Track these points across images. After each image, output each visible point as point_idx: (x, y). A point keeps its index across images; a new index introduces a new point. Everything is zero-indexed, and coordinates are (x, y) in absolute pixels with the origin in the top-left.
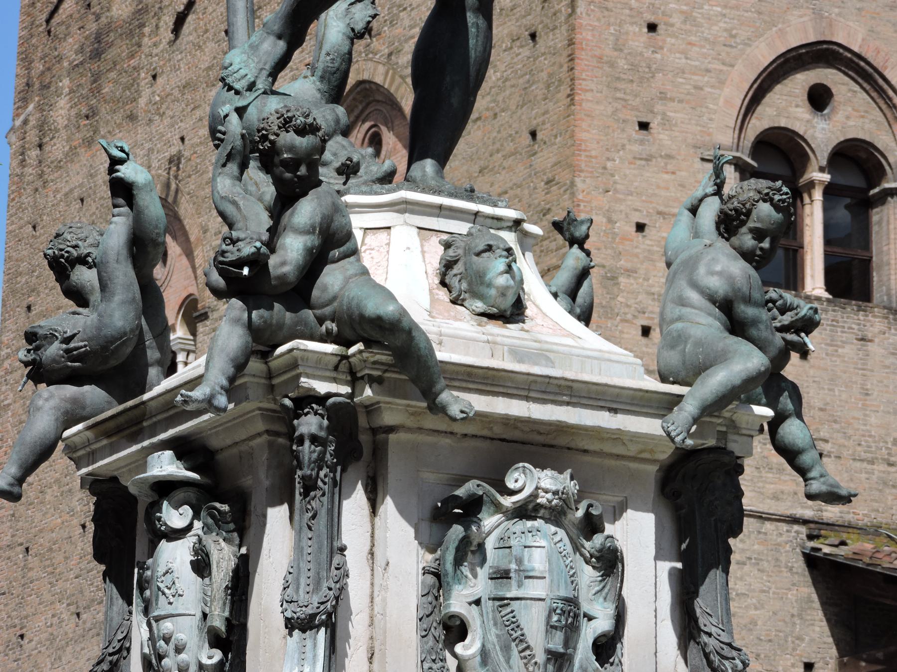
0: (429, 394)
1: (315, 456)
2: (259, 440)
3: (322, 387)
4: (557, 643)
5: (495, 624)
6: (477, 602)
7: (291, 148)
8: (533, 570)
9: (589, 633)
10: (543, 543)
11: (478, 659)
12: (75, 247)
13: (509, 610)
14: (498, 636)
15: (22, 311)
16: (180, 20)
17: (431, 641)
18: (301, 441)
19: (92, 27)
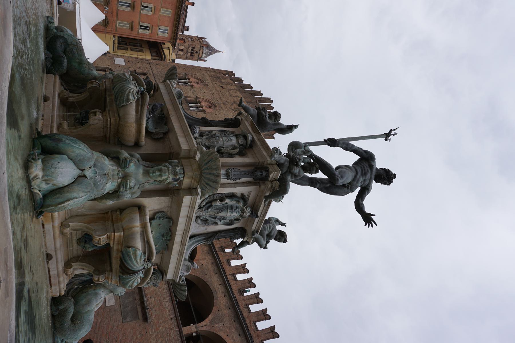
1: (259, 175)
2: (257, 160)
3: (271, 176)
5: (222, 207)
7: (313, 170)
8: (232, 213)
9: (218, 221)
10: (237, 215)
11: (216, 204)
12: (278, 117)
13: (225, 209)
14: (220, 207)
15: (191, 67)
16: (222, 87)
18: (262, 172)
19: (221, 77)
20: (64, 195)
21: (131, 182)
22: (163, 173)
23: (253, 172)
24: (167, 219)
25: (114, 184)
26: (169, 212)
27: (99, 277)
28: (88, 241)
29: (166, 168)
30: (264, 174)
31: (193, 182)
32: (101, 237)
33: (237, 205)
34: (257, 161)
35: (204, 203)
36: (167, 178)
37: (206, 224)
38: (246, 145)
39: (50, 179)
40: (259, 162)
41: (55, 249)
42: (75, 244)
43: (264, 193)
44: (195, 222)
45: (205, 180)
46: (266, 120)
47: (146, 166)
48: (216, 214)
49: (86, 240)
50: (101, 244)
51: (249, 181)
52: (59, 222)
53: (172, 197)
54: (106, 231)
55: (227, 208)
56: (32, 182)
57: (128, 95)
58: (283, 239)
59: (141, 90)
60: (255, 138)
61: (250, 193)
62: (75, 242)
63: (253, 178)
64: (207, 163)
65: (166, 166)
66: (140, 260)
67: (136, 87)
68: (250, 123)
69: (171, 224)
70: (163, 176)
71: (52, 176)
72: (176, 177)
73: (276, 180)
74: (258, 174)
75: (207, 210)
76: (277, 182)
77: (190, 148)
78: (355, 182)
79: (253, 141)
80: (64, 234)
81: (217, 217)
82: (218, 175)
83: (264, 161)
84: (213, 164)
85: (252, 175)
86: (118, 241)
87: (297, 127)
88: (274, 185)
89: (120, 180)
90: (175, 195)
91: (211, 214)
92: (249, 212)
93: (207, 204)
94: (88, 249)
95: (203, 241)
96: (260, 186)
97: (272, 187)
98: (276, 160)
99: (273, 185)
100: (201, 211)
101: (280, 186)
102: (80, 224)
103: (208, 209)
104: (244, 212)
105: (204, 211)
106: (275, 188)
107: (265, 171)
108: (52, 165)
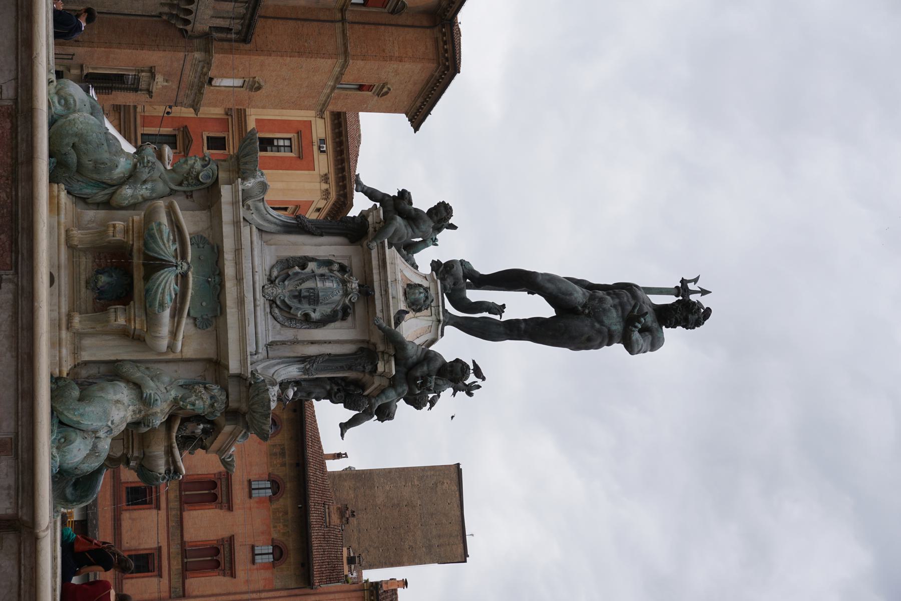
0: (374, 239)
3: (370, 219)
4: (304, 293)
6: (313, 272)
8: (326, 282)
11: (295, 271)
25: (129, 162)
26: (211, 236)
27: (115, 308)
31: (231, 177)
35: (275, 273)
39: (62, 87)
41: (59, 267)
44: (269, 316)
48: (298, 286)
55: (313, 276)
58: (461, 365)
62: (83, 283)
66: (168, 242)
78: (597, 302)
86: (139, 232)
91: (290, 289)
92: (357, 280)
96: (362, 246)
100: (274, 287)
103: (283, 281)
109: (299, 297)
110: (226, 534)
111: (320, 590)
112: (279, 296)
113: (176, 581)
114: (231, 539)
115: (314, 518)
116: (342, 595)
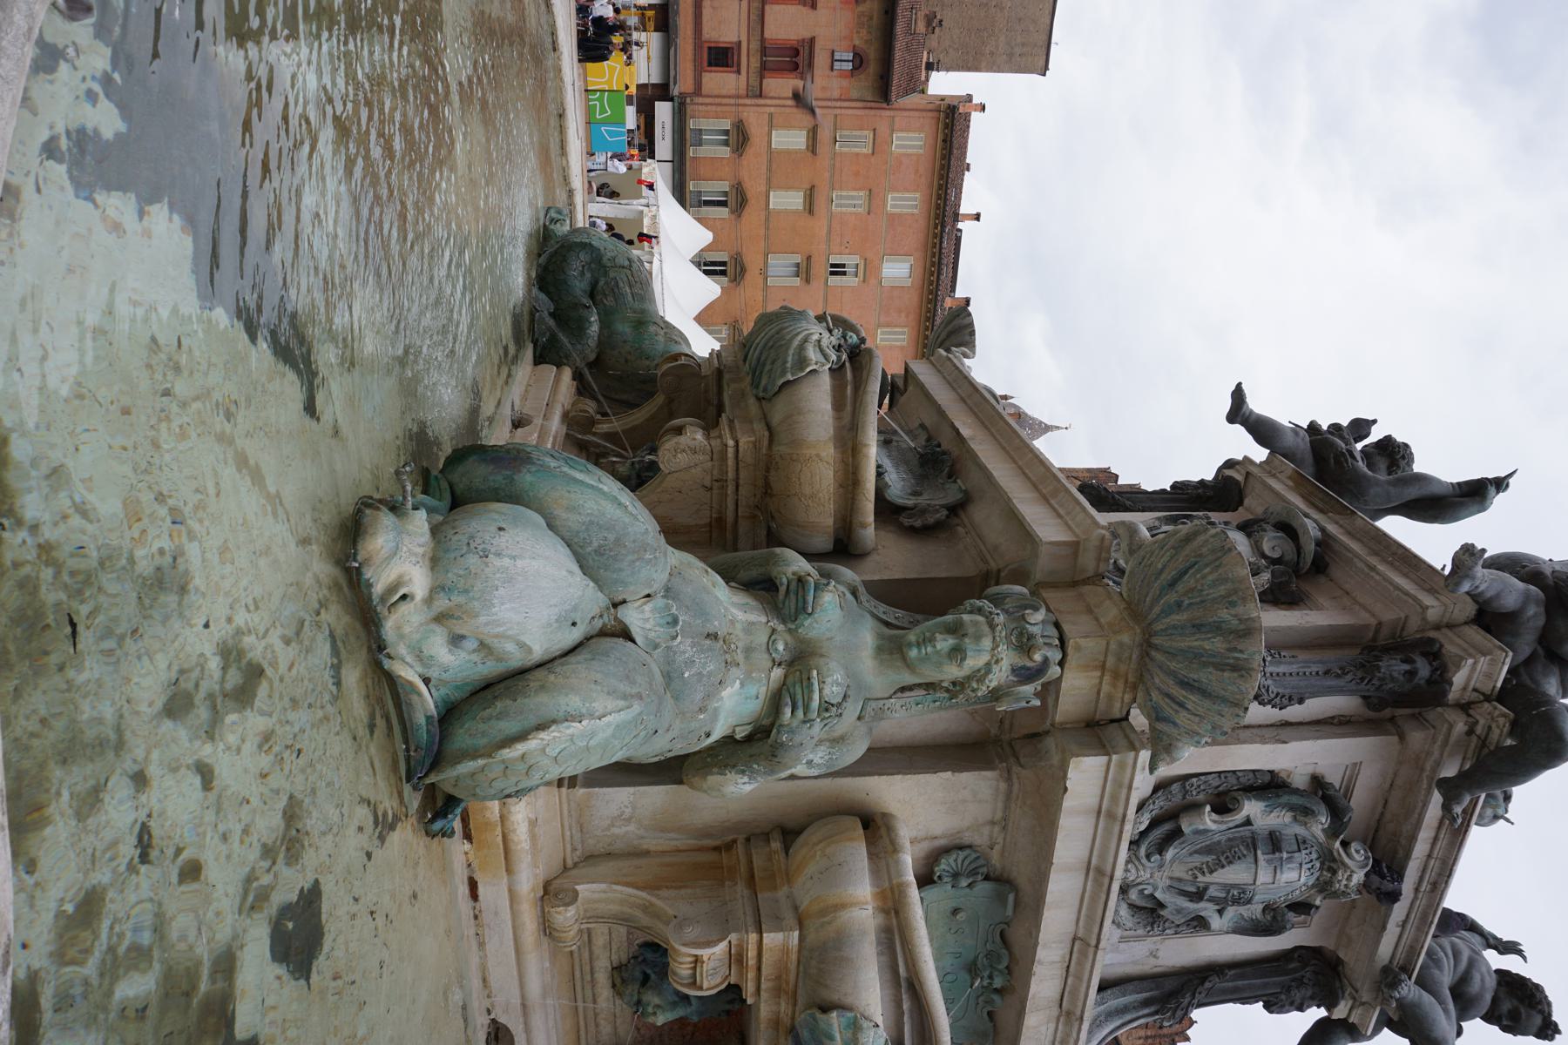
1: (1395, 674)
3: (1459, 679)
4: (1213, 892)
5: (1230, 840)
6: (1248, 822)
8: (1282, 872)
10: (1303, 879)
11: (1201, 827)
12: (1403, 457)
14: (1219, 842)
17: (1216, 783)
20: (527, 700)
21: (829, 680)
22: (967, 640)
23: (1363, 666)
24: (987, 886)
25: (752, 690)
26: (997, 848)
28: (653, 976)
29: (981, 619)
30: (1424, 670)
31: (1106, 688)
32: (705, 953)
33: (1299, 830)
34: (1363, 618)
36: (988, 664)
37: (1152, 925)
38: (1298, 563)
40: (1380, 624)
41: (524, 1006)
42: (605, 992)
43: (1428, 767)
45: (1173, 665)
46: (1355, 470)
47: (887, 624)
48: (1203, 873)
49: (649, 971)
50: (705, 985)
51: (1345, 712)
52: (537, 875)
53: (1009, 771)
54: (722, 925)
55: (1249, 844)
56: (385, 618)
57: (802, 348)
59: (850, 341)
60: (1332, 528)
61: (1353, 771)
62: (602, 978)
63: (1364, 697)
64: (1172, 584)
65: (980, 611)
67: (830, 331)
68: (1291, 484)
69: (1010, 912)
70: (969, 654)
71: (466, 591)
72: (1031, 659)
73: (1488, 698)
74: (1394, 667)
75: (1158, 857)
76: (1496, 708)
77: (1076, 536)
79: (1325, 542)
80: (557, 934)
81: (1206, 889)
82: (1242, 627)
83: (1403, 615)
84: (1210, 578)
85: (1362, 679)
86: (778, 978)
87: (1507, 486)
88: (1482, 722)
89: (778, 673)
90: (1022, 760)
91: (1177, 874)
93: (1154, 824)
94: (655, 1014)
95: (1141, 1013)
97: (1470, 732)
98: (1482, 592)
99: (1477, 722)
101: (1514, 724)
102: (621, 893)
103: (1161, 848)
104: (1335, 866)
105: (1144, 860)
106: (1488, 734)
107: (1424, 654)
108: (472, 537)
109: (1198, 895)
110: (807, 35)
111: (896, 105)
112: (1141, 887)
113: (754, 81)
114: (812, 40)
115: (900, 28)
116: (917, 114)
